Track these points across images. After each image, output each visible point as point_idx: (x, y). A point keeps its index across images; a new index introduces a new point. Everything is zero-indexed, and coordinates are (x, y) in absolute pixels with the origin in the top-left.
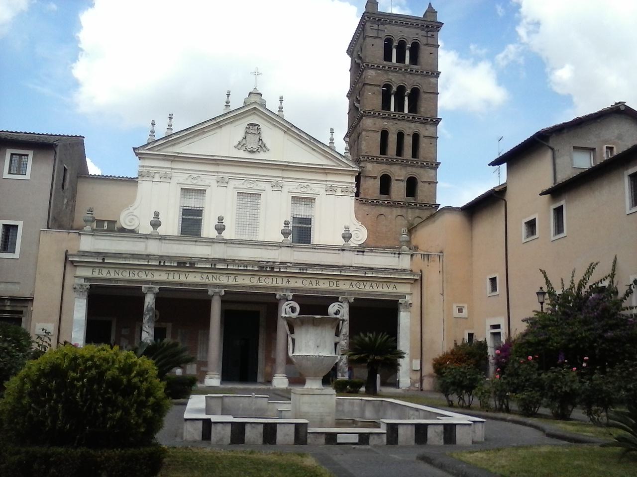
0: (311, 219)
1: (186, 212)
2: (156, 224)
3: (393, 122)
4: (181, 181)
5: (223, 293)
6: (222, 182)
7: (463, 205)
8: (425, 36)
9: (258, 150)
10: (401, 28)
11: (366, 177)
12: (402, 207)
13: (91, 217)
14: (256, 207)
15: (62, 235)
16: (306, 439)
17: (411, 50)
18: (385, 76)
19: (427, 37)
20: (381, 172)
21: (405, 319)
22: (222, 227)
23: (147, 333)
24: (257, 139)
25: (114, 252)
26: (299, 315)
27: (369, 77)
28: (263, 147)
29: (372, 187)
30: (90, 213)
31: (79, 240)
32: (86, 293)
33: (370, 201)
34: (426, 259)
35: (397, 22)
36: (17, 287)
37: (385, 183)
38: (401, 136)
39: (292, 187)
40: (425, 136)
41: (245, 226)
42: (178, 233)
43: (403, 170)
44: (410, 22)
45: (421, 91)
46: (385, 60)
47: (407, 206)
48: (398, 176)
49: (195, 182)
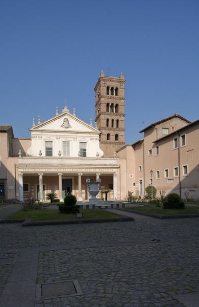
1: (47, 149)
6: (58, 138)
14: (68, 146)
17: (115, 90)
21: (115, 180)
28: (69, 126)
29: (104, 137)
37: (108, 135)
38: (113, 120)
39: (81, 138)
47: (115, 143)
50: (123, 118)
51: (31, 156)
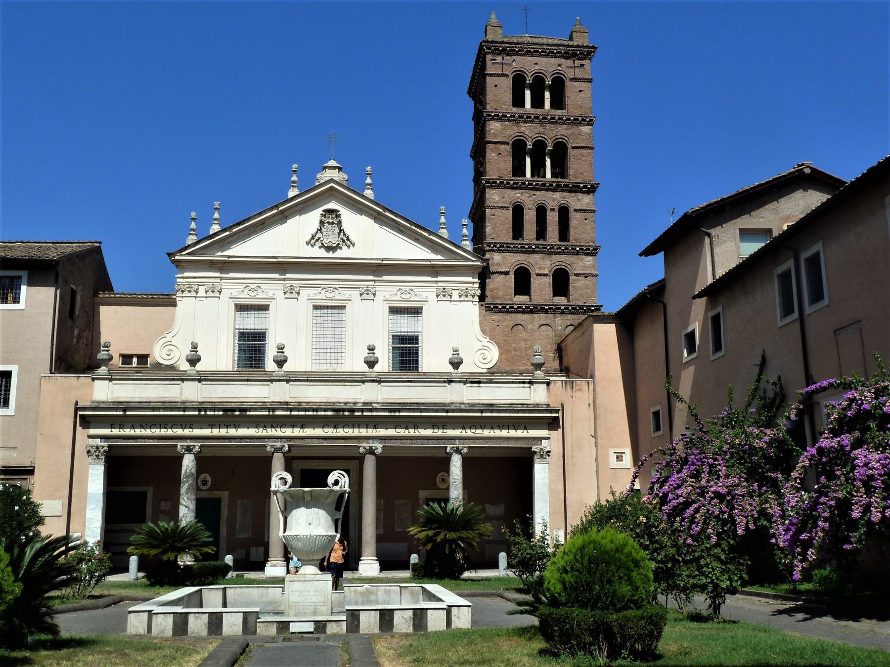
0: (417, 336)
2: (193, 361)
3: (528, 193)
4: (235, 294)
5: (286, 448)
6: (292, 293)
7: (620, 308)
8: (572, 67)
9: (339, 244)
10: (536, 59)
11: (494, 273)
12: (546, 312)
13: (107, 355)
14: (339, 324)
15: (69, 380)
16: (256, 630)
18: (515, 128)
19: (575, 67)
20: (515, 264)
22: (283, 358)
23: (186, 507)
24: (337, 230)
25: (139, 400)
26: (290, 487)
27: (492, 131)
28: (347, 241)
30: (106, 349)
31: (92, 387)
32: (103, 457)
33: (500, 307)
34: (569, 387)
35: (530, 51)
36: (14, 454)
38: (541, 212)
40: (575, 210)
41: (325, 351)
42: (233, 367)
43: (546, 260)
44: (548, 49)
45: (569, 146)
46: (514, 105)
48: (541, 268)
49: (253, 294)
50: (585, 200)
51: (171, 367)
